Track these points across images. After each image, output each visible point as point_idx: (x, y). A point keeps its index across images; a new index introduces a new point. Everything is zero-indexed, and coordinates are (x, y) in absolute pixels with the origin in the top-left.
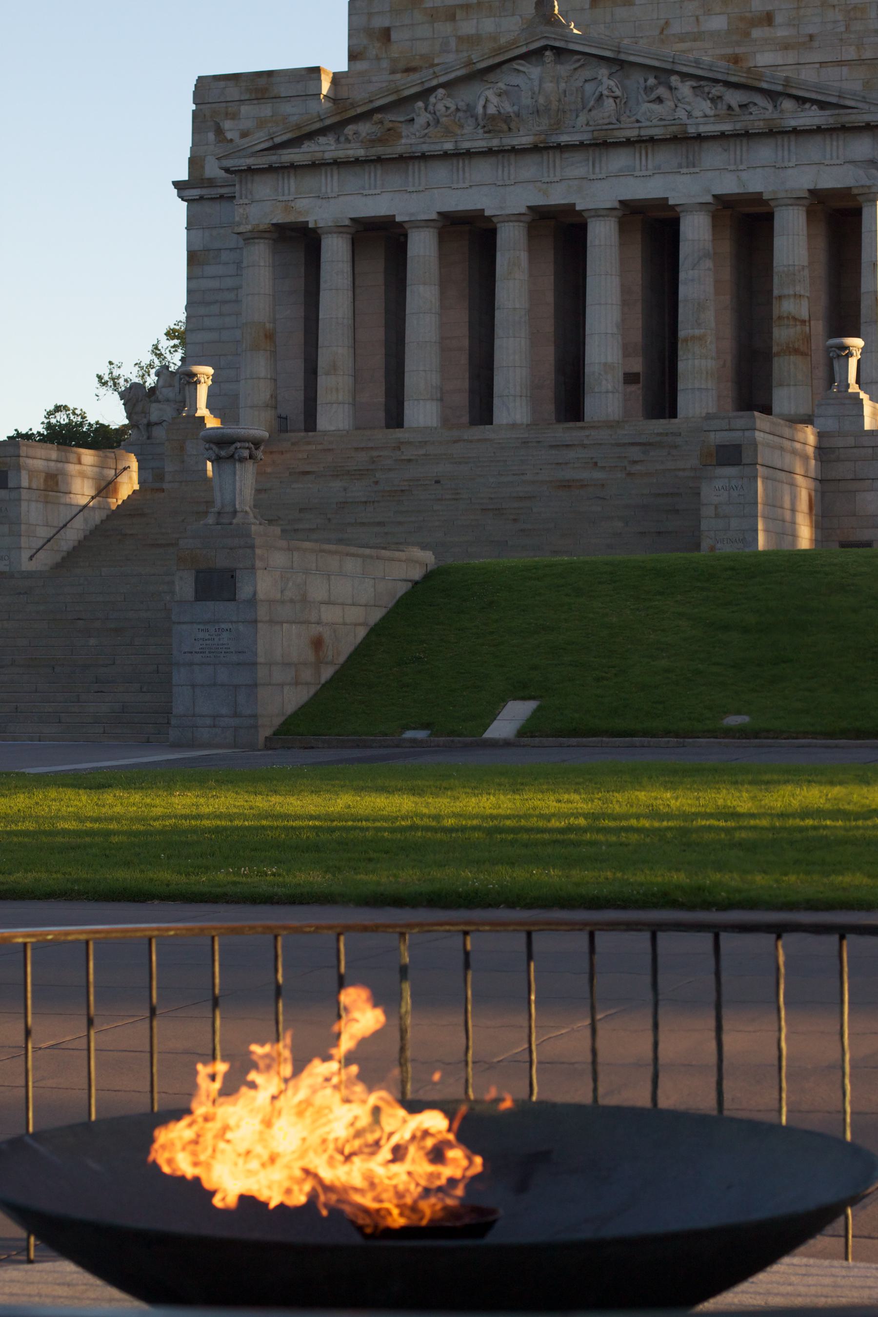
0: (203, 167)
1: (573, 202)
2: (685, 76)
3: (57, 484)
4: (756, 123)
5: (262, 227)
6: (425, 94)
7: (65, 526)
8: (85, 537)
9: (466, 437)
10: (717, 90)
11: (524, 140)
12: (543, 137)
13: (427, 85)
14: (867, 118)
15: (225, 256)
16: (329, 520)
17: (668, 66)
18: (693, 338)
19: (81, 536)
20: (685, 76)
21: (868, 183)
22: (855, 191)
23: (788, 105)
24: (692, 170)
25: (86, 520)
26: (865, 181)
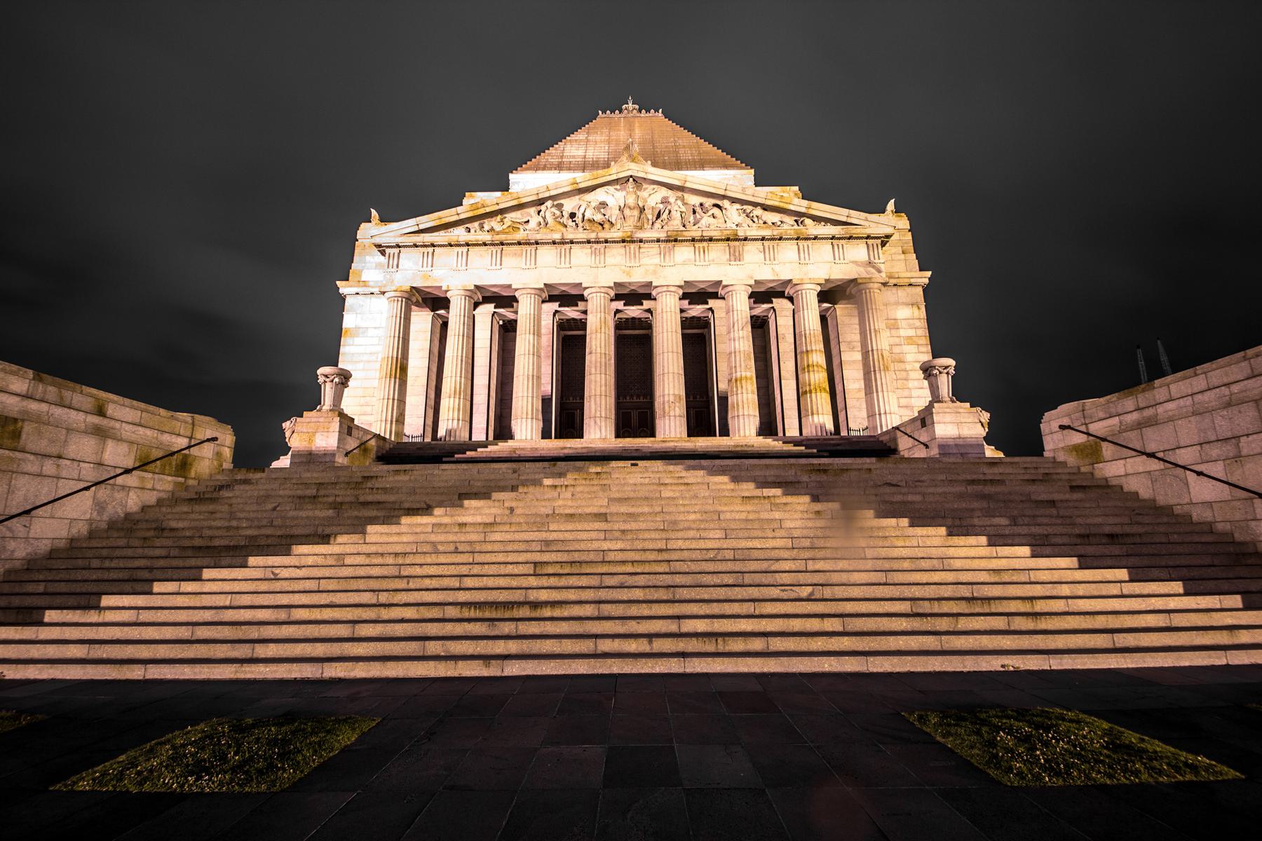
0: (360, 276)
1: (650, 280)
2: (734, 201)
3: (17, 435)
4: (789, 232)
5: (403, 289)
6: (541, 202)
7: (27, 512)
8: (92, 535)
9: (569, 446)
10: (758, 211)
11: (615, 234)
12: (629, 234)
13: (541, 196)
14: (868, 231)
15: (371, 332)
16: (512, 510)
17: (722, 192)
18: (746, 378)
19: (82, 529)
20: (734, 201)
21: (868, 276)
22: (860, 281)
23: (808, 221)
24: (738, 263)
25: (100, 506)
26: (864, 275)
